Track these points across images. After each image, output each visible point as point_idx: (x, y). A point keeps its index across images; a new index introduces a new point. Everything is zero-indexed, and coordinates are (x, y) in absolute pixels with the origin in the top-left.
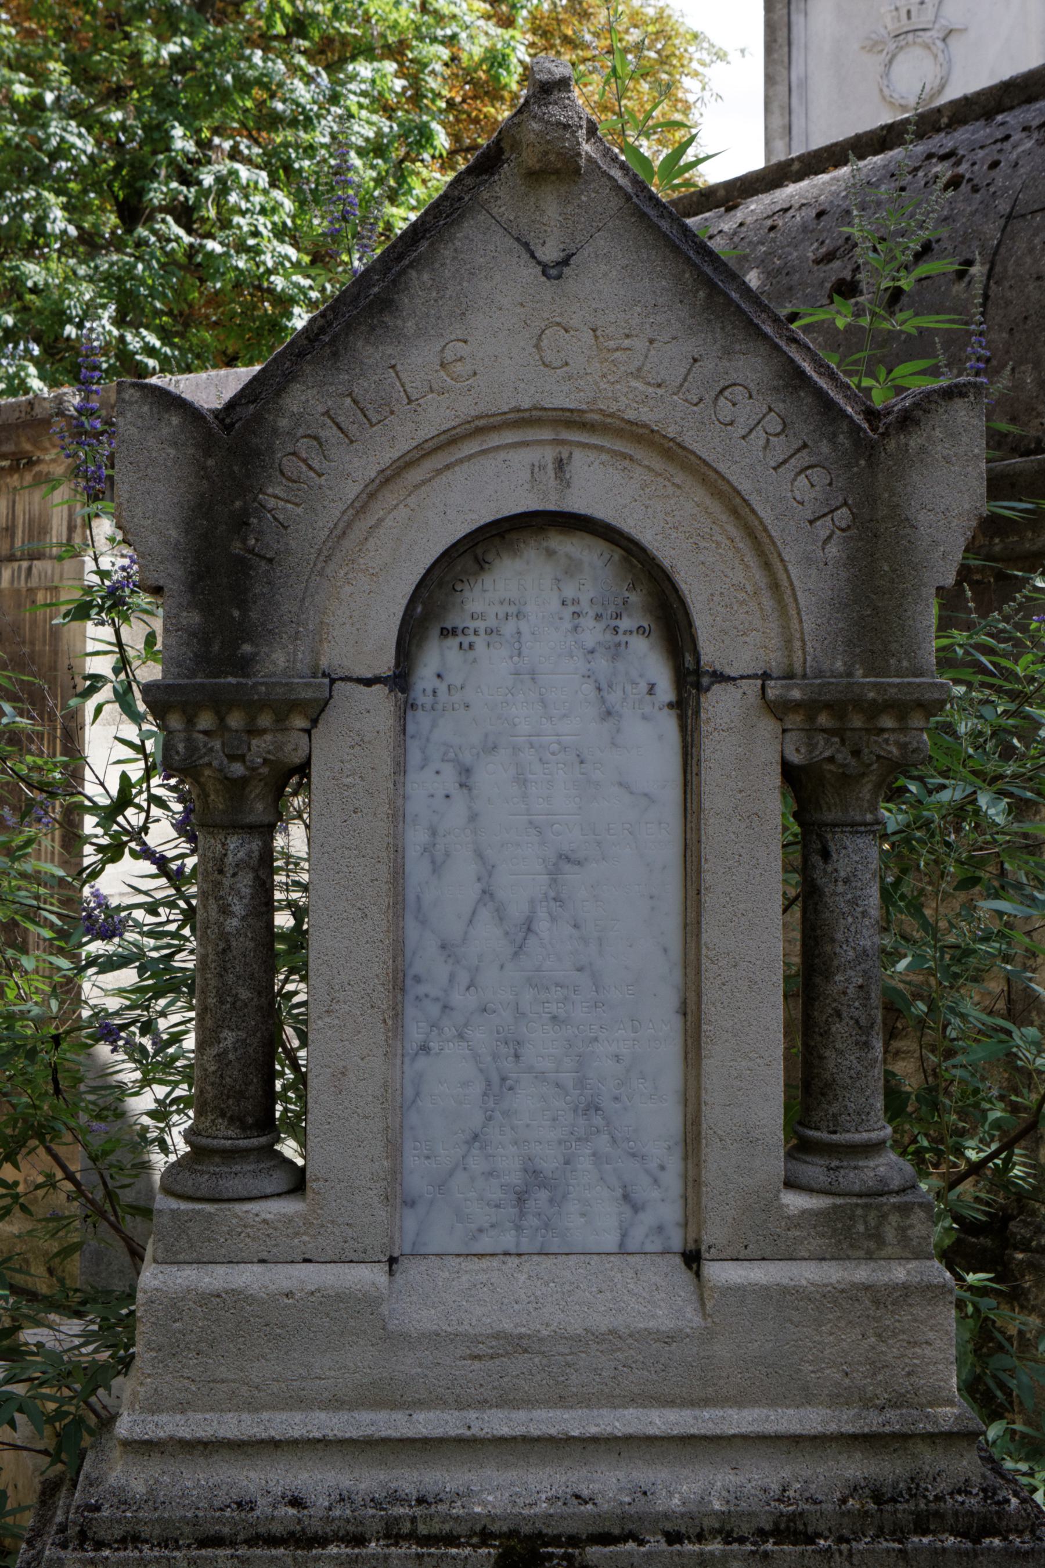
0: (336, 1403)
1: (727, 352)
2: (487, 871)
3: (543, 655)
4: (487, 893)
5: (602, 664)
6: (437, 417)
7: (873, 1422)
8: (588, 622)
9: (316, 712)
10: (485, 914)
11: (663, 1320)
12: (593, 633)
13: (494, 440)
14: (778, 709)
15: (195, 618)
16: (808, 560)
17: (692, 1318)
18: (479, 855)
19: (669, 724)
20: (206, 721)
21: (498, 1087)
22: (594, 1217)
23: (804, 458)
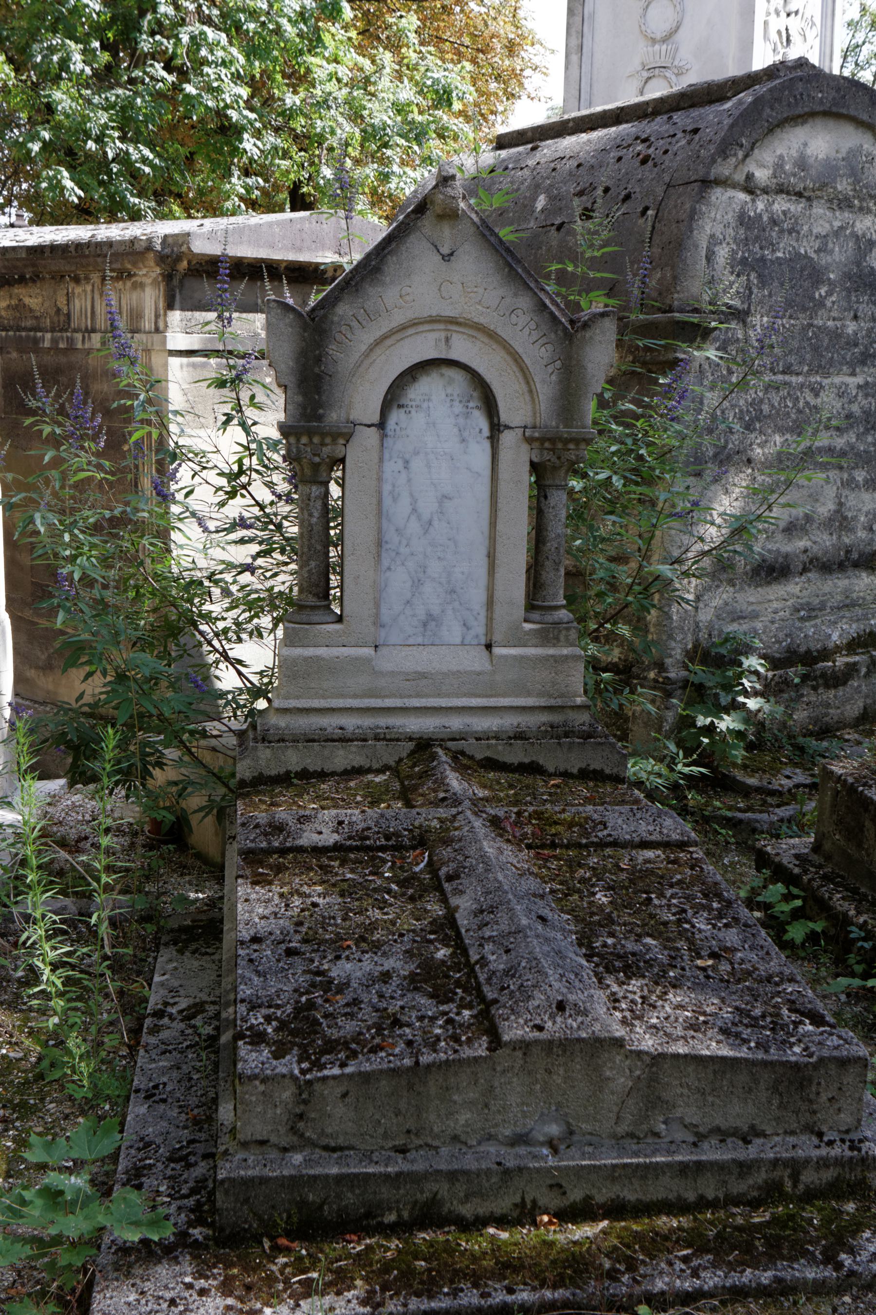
0: (355, 696)
1: (516, 295)
2: (414, 501)
3: (438, 417)
4: (414, 510)
5: (461, 420)
6: (399, 318)
7: (552, 702)
8: (456, 403)
9: (348, 437)
10: (413, 518)
11: (477, 667)
12: (458, 408)
13: (421, 328)
14: (529, 440)
15: (300, 399)
16: (543, 381)
17: (488, 667)
18: (411, 495)
19: (487, 445)
20: (304, 440)
21: (417, 584)
22: (453, 632)
23: (544, 340)
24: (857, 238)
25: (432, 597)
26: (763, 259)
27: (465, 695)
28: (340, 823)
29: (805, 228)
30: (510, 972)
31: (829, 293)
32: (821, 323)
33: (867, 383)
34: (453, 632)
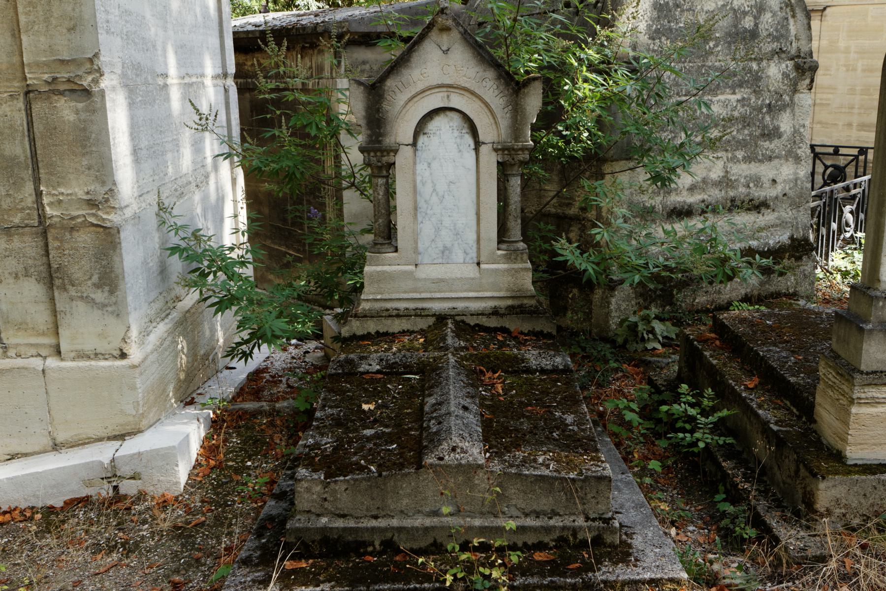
0: (405, 292)
1: (485, 71)
2: (434, 185)
4: (434, 190)
5: (458, 140)
6: (420, 86)
7: (514, 294)
8: (455, 131)
9: (396, 151)
10: (434, 194)
11: (472, 275)
12: (456, 133)
13: (433, 91)
14: (496, 150)
15: (369, 132)
16: (502, 117)
17: (478, 275)
18: (433, 182)
19: (473, 153)
20: (372, 154)
21: (438, 230)
22: (458, 256)
23: (502, 95)
24: (735, 11)
25: (446, 237)
26: (670, 29)
27: (465, 291)
28: (382, 360)
29: (699, 7)
30: (437, 433)
31: (716, 46)
32: (710, 64)
33: (744, 99)
34: (458, 256)
